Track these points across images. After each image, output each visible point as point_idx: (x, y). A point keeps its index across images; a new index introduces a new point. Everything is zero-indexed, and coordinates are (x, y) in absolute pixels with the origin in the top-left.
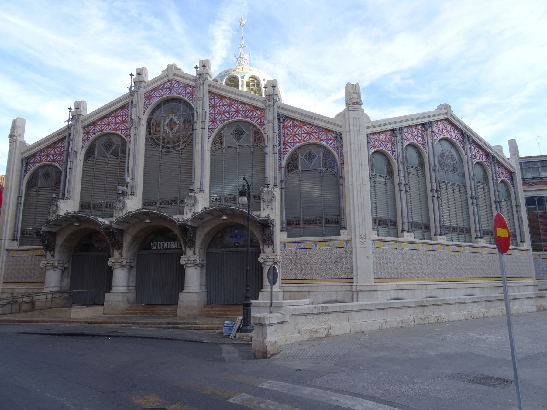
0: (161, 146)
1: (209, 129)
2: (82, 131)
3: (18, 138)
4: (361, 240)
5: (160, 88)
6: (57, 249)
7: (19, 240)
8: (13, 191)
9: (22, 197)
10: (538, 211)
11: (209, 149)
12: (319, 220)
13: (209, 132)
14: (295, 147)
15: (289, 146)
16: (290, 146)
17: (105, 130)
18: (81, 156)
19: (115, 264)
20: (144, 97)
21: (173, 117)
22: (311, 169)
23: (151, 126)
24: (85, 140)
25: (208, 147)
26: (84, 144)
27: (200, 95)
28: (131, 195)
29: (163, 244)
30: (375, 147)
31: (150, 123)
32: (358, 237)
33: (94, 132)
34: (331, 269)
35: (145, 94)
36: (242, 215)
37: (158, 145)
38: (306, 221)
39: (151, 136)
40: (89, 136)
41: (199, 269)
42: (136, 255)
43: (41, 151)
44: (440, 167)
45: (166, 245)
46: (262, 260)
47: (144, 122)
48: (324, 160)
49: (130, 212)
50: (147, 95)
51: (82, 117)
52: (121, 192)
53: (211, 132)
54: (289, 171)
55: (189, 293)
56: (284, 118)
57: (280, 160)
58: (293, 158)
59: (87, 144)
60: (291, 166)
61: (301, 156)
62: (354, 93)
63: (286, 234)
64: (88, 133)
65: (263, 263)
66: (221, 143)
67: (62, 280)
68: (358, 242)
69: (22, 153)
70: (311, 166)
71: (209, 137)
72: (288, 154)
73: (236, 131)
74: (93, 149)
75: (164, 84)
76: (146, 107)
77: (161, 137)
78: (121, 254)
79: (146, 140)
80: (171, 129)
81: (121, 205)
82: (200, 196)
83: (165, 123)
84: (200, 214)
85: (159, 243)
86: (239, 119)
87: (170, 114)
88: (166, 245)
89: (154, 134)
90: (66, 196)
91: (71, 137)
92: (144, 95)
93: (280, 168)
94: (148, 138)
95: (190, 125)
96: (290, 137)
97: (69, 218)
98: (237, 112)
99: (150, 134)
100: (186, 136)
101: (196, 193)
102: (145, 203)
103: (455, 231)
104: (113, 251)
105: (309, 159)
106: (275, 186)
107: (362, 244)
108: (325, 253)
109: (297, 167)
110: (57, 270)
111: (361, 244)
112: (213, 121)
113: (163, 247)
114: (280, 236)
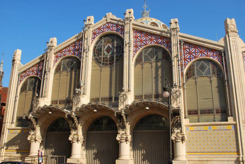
0: (102, 63)
1: (133, 51)
2: (54, 55)
3: (17, 61)
5: (102, 28)
7: (15, 123)
8: (13, 93)
9: (17, 96)
11: (133, 64)
12: (211, 110)
13: (133, 53)
15: (187, 61)
16: (188, 60)
17: (67, 54)
18: (53, 71)
20: (91, 33)
21: (110, 45)
22: (204, 76)
23: (96, 51)
24: (55, 61)
25: (133, 63)
26: (55, 64)
27: (126, 29)
28: (83, 94)
31: (95, 49)
33: (61, 56)
35: (92, 31)
36: (159, 107)
37: (100, 63)
38: (202, 111)
39: (95, 57)
40: (58, 59)
42: (86, 134)
43: (29, 69)
46: (174, 138)
47: (91, 49)
48: (213, 69)
49: (84, 105)
50: (93, 32)
51: (54, 47)
52: (77, 92)
53: (134, 53)
55: (122, 160)
56: (184, 43)
57: (182, 70)
58: (191, 69)
59: (57, 64)
60: (189, 74)
61: (197, 67)
63: (188, 120)
64: (57, 57)
65: (175, 140)
66: (141, 60)
69: (19, 70)
70: (203, 74)
71: (133, 56)
72: (187, 66)
73: (151, 52)
74: (60, 66)
75: (104, 25)
76: (93, 40)
77: (102, 58)
79: (93, 60)
80: (108, 52)
82: (128, 94)
83: (104, 49)
84: (131, 106)
86: (152, 44)
87: (108, 43)
89: (98, 56)
90: (43, 96)
91: (47, 59)
92: (91, 32)
93: (182, 75)
94: (94, 59)
95: (121, 50)
96: (188, 55)
97: (46, 109)
98: (151, 40)
99: (95, 56)
100: (118, 57)
101: (126, 92)
102: (92, 100)
105: (202, 69)
106: (179, 87)
108: (218, 134)
109: (194, 75)
112: (136, 46)
114: (185, 122)
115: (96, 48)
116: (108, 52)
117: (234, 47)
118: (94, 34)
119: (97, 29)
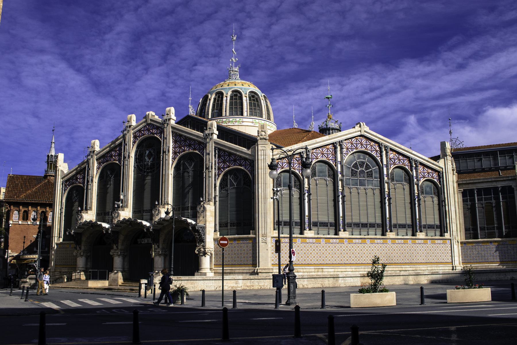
0: (143, 171)
2: (96, 162)
4: (263, 238)
6: (83, 244)
9: (63, 208)
10: (493, 201)
14: (225, 170)
19: (114, 254)
29: (145, 240)
30: (283, 168)
32: (260, 236)
34: (244, 257)
41: (162, 257)
44: (353, 175)
45: (146, 241)
54: (221, 189)
59: (100, 171)
60: (223, 185)
61: (230, 177)
62: (262, 131)
67: (86, 264)
68: (260, 239)
71: (172, 164)
78: (117, 247)
81: (116, 215)
85: (142, 239)
88: (146, 241)
94: (136, 166)
103: (365, 227)
104: (113, 245)
107: (264, 240)
110: (83, 257)
111: (262, 241)
112: (175, 153)
113: (145, 242)
115: (137, 153)
116: (150, 159)
117: (262, 156)
118: (135, 137)
119: (138, 131)
